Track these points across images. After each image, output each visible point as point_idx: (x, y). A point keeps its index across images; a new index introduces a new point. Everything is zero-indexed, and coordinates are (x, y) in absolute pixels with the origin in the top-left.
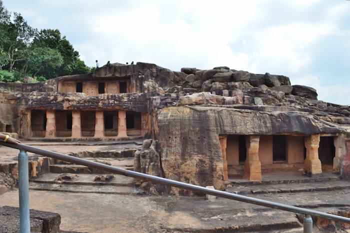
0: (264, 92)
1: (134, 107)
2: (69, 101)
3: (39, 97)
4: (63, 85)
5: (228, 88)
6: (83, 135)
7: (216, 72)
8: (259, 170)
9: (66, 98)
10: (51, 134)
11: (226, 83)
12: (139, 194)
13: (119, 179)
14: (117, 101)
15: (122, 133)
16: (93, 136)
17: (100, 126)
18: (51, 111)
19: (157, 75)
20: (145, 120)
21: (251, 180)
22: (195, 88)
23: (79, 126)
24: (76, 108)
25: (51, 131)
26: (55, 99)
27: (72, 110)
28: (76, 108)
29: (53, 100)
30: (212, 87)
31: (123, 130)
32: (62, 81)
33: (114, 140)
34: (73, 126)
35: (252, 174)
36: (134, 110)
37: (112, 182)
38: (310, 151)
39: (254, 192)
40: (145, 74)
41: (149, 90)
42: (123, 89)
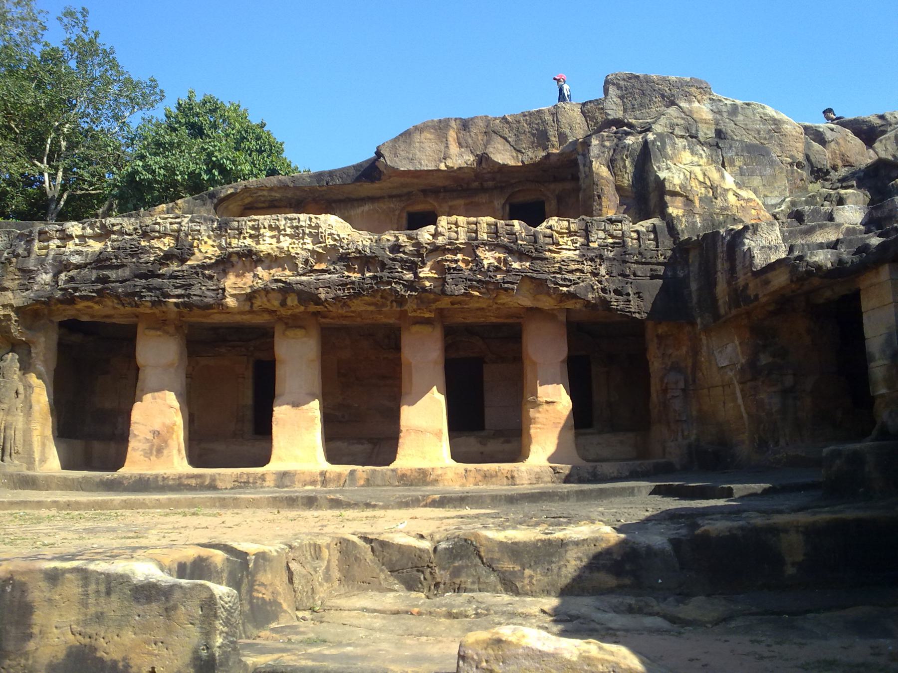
2: (251, 259)
3: (96, 246)
10: (159, 451)
14: (521, 255)
16: (393, 459)
18: (160, 324)
19: (719, 133)
20: (676, 368)
25: (156, 433)
26: (181, 253)
28: (292, 301)
29: (168, 257)
41: (689, 201)
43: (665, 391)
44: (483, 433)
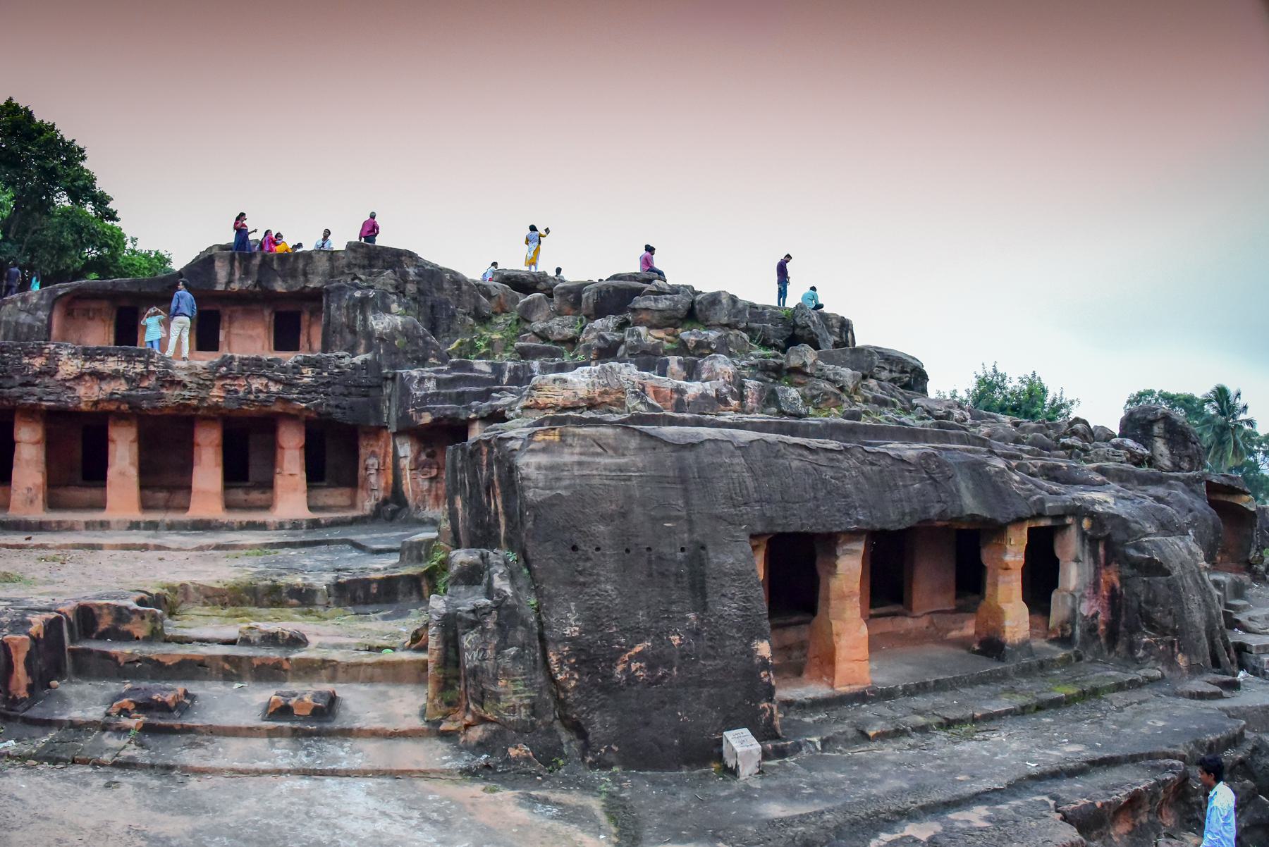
0: (808, 370)
1: (337, 406)
4: (69, 314)
5: (682, 348)
6: (145, 506)
7: (639, 292)
8: (863, 651)
9: (88, 365)
11: (671, 330)
12: (470, 773)
13: (360, 704)
14: (277, 381)
15: (291, 500)
17: (207, 474)
18: (32, 413)
21: (843, 689)
22: (556, 342)
23: (133, 472)
24: (124, 407)
26: (50, 372)
27: (111, 412)
29: (41, 374)
30: (622, 342)
31: (295, 490)
32: (66, 299)
33: (262, 526)
34: (112, 473)
35: (842, 667)
36: (338, 414)
37: (336, 725)
38: (1001, 578)
39: (871, 733)
40: (378, 286)
42: (286, 337)
43: (366, 469)
44: (248, 484)
